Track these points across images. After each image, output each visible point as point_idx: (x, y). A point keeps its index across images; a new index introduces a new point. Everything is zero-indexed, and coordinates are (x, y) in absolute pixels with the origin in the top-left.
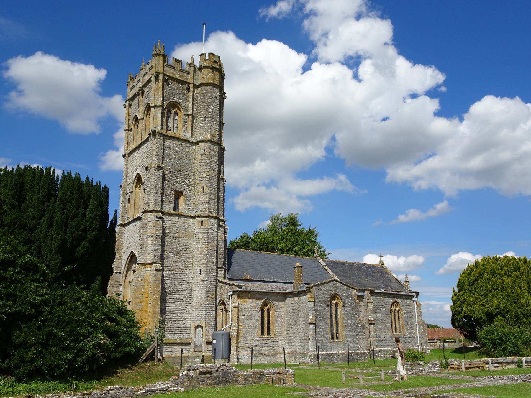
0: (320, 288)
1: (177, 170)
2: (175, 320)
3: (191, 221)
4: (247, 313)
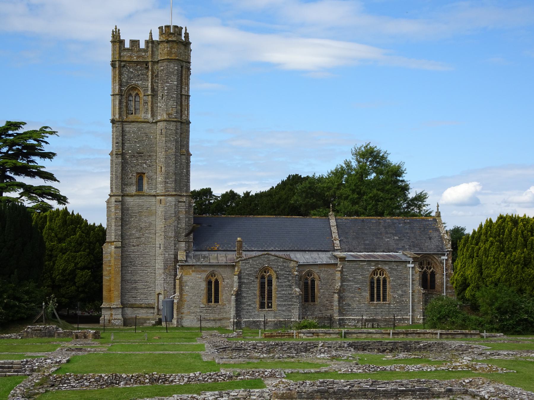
0: (248, 262)
1: (138, 153)
2: (140, 288)
3: (153, 199)
4: (191, 284)
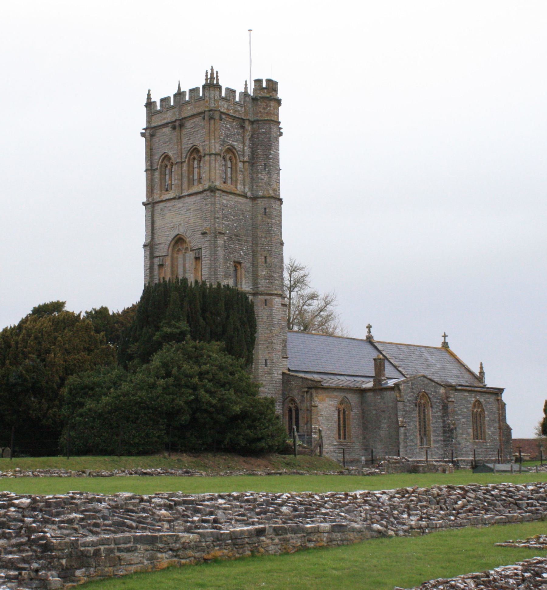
1: (235, 235)
